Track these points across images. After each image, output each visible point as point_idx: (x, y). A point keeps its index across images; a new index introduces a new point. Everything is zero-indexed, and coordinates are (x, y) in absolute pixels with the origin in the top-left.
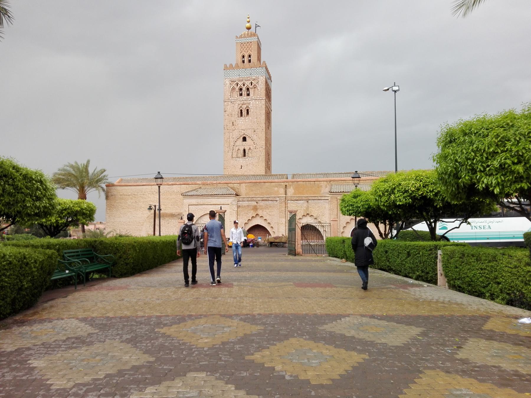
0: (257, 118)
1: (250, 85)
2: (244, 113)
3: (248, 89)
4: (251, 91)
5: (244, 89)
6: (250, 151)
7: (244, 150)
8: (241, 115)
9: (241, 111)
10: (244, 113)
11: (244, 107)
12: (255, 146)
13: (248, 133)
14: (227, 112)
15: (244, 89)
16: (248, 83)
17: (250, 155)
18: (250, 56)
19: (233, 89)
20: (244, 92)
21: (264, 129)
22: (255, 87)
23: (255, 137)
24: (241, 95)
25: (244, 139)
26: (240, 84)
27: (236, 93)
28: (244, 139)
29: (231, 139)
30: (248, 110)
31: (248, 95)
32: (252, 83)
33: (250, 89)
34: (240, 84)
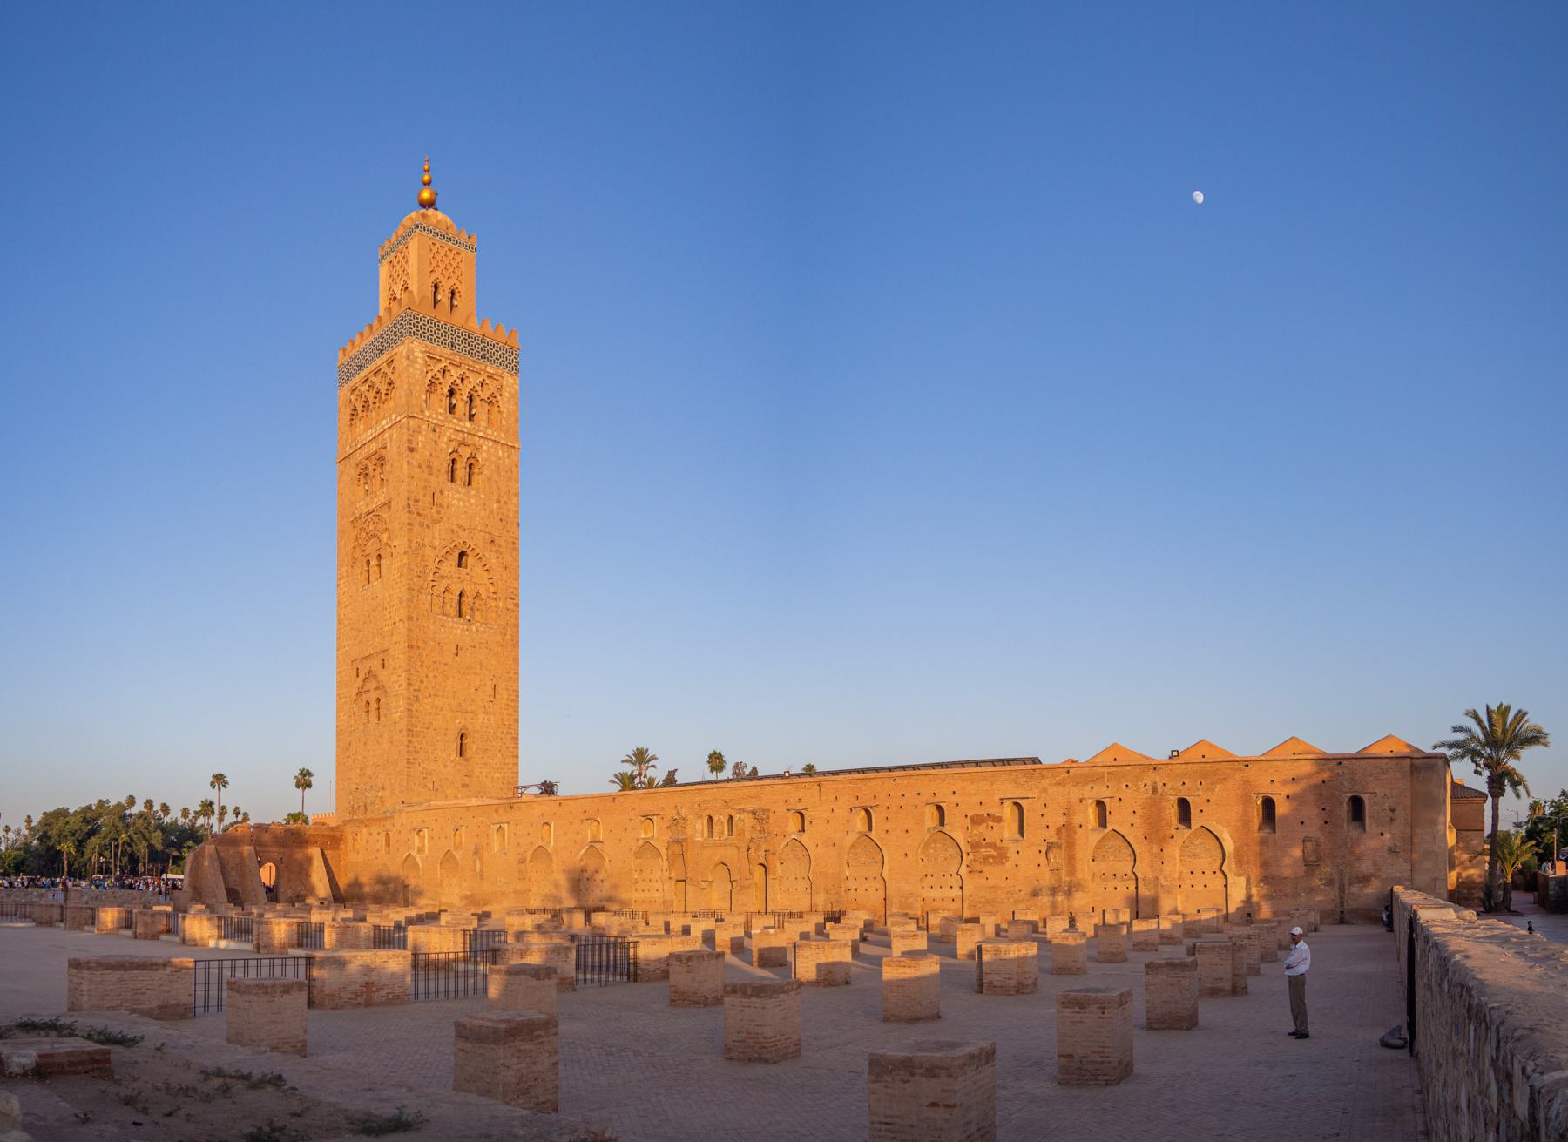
2: (461, 472)
4: (480, 409)
6: (478, 602)
9: (453, 461)
10: (461, 472)
11: (466, 452)
12: (492, 589)
13: (476, 542)
14: (415, 455)
16: (475, 380)
20: (462, 408)
24: (452, 408)
27: (440, 403)
29: (428, 551)
31: (471, 417)
34: (455, 373)
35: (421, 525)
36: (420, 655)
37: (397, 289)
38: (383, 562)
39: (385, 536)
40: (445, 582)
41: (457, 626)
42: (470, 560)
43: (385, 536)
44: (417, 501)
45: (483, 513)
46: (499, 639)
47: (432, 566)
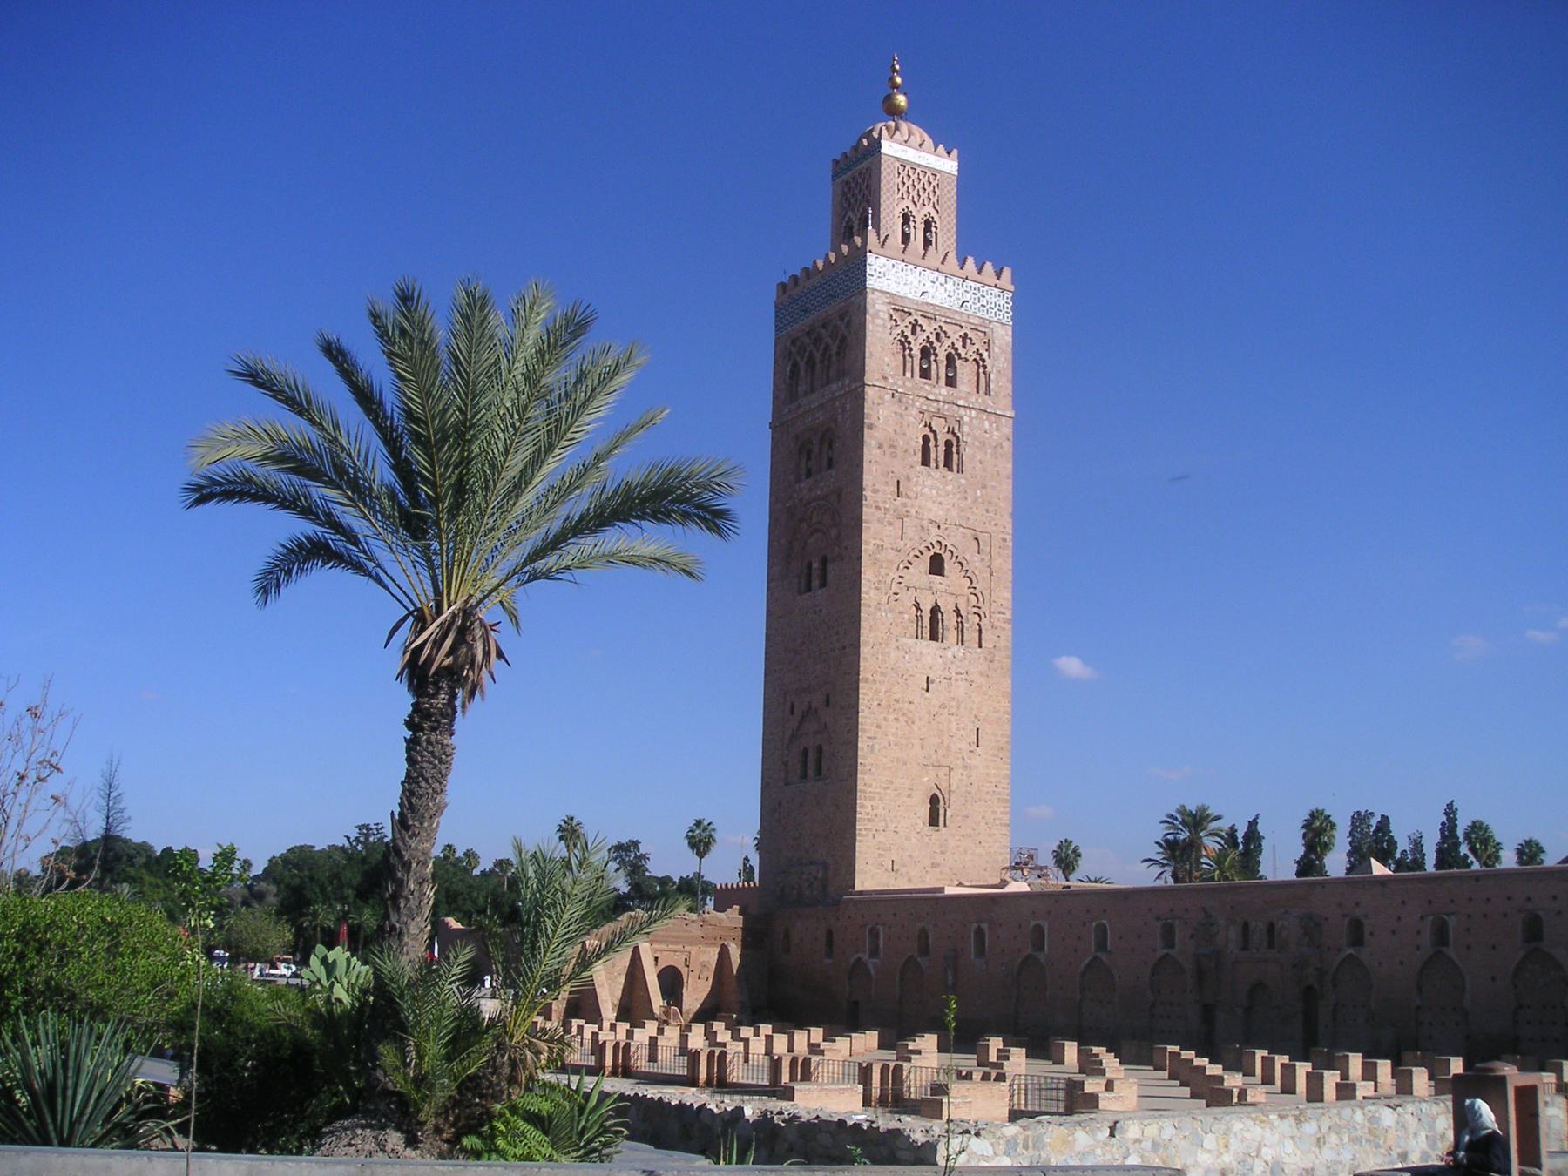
0: (984, 487)
1: (959, 345)
2: (938, 453)
3: (950, 358)
4: (965, 371)
5: (942, 354)
7: (935, 610)
8: (925, 462)
9: (926, 439)
10: (938, 453)
13: (956, 540)
15: (942, 354)
16: (955, 336)
17: (951, 636)
18: (928, 225)
19: (904, 344)
20: (939, 368)
21: (1009, 537)
22: (980, 362)
23: (975, 563)
24: (925, 374)
25: (937, 566)
26: (929, 328)
28: (937, 566)
30: (948, 444)
31: (951, 382)
32: (965, 338)
33: (958, 363)
35: (880, 521)
36: (877, 692)
37: (854, 217)
38: (830, 567)
39: (834, 532)
40: (912, 593)
41: (927, 647)
42: (948, 565)
43: (834, 532)
44: (875, 491)
45: (963, 504)
46: (983, 666)
47: (894, 575)
